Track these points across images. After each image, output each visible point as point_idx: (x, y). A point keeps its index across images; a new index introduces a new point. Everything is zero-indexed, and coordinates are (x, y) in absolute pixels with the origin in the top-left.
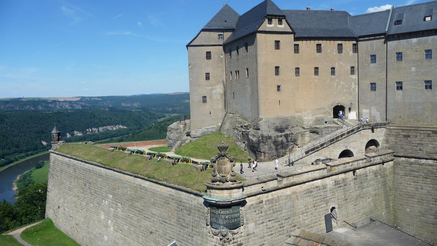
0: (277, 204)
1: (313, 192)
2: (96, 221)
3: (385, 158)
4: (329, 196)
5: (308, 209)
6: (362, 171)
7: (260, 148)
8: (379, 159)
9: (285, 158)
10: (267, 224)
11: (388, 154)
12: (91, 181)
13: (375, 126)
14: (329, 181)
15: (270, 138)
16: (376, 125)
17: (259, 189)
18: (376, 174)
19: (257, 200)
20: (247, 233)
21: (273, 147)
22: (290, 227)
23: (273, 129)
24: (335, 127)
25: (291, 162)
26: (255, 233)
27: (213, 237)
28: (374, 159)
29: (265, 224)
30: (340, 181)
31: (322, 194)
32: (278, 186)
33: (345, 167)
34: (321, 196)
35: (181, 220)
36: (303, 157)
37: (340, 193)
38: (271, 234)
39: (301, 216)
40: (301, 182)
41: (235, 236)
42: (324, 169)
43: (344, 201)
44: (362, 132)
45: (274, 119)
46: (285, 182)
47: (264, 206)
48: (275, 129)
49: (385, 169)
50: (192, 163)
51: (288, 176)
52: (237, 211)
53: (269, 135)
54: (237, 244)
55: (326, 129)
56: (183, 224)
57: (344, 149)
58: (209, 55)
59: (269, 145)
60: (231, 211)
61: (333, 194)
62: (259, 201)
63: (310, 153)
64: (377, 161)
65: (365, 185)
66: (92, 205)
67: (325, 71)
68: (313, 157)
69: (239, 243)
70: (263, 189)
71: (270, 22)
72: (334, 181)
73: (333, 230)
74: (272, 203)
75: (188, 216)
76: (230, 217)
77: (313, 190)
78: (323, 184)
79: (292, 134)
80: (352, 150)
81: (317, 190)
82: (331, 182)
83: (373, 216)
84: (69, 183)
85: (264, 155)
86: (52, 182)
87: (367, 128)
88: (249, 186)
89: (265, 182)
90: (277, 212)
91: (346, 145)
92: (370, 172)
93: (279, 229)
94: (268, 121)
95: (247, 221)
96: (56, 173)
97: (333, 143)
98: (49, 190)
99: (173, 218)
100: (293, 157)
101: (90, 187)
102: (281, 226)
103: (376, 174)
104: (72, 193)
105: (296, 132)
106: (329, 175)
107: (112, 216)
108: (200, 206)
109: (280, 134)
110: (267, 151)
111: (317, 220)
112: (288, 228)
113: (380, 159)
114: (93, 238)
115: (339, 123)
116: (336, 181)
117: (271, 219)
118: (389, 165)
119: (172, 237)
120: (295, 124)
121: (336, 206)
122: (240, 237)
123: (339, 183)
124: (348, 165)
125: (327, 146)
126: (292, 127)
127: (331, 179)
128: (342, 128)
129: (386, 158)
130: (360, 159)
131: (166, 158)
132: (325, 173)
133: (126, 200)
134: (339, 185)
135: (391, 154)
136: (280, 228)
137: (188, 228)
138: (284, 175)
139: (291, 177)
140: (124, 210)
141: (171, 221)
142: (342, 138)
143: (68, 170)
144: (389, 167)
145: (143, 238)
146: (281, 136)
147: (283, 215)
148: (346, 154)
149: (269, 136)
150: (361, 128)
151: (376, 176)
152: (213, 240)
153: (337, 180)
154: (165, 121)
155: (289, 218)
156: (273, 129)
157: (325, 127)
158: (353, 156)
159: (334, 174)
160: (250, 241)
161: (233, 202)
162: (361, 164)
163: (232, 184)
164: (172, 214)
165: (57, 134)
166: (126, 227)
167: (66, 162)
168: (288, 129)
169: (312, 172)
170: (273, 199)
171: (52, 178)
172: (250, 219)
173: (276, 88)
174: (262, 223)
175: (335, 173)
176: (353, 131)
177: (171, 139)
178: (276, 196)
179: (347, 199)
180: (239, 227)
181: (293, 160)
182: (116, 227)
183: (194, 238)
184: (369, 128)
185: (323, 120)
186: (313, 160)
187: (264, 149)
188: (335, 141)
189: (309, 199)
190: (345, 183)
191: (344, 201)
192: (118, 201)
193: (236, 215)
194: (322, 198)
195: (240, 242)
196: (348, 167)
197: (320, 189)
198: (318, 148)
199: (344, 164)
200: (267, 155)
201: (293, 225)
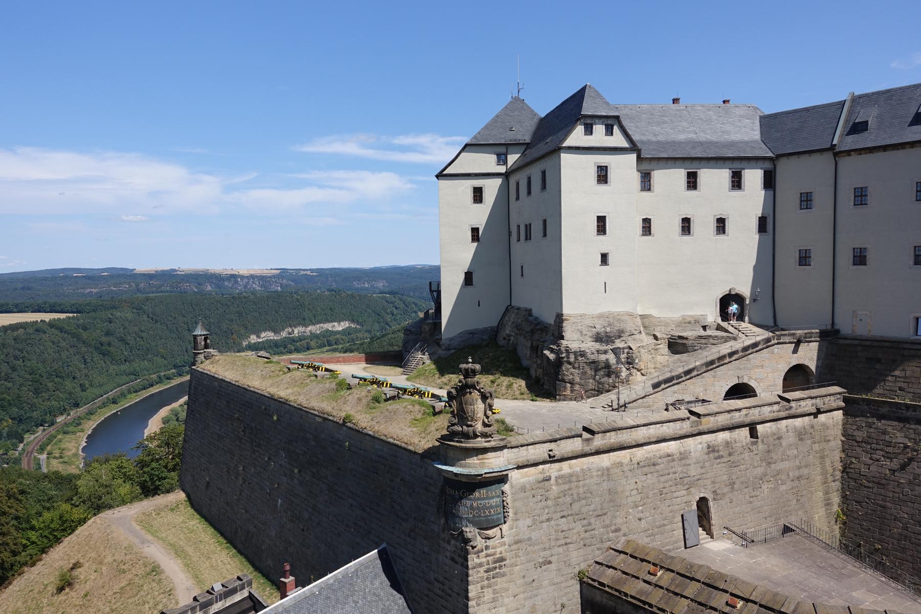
0: (581, 483)
1: (658, 464)
3: (824, 404)
4: (695, 474)
5: (648, 497)
6: (770, 428)
7: (564, 375)
8: (810, 405)
9: (612, 396)
10: (558, 523)
11: (830, 395)
13: (805, 338)
14: (695, 445)
15: (583, 354)
16: (808, 335)
17: (544, 453)
18: (802, 435)
19: (538, 474)
20: (516, 538)
21: (590, 372)
22: (608, 532)
24: (723, 337)
25: (622, 402)
26: (531, 539)
27: (449, 543)
28: (799, 404)
29: (553, 523)
30: (718, 446)
31: (680, 469)
32: (582, 450)
33: (732, 417)
34: (675, 473)
36: (648, 394)
37: (720, 471)
38: (566, 544)
39: (631, 510)
40: (634, 443)
41: (490, 543)
42: (683, 420)
43: (726, 485)
44: (776, 349)
45: (593, 318)
46: (599, 441)
47: (554, 487)
49: (824, 425)
50: (431, 397)
51: (605, 432)
52: (496, 493)
53: (582, 349)
54: (494, 558)
55: (703, 341)
57: (735, 381)
58: (478, 195)
59: (581, 367)
60: (483, 492)
61: (703, 471)
62: (541, 477)
63: (663, 386)
64: (806, 409)
65: (774, 456)
67: (704, 226)
68: (670, 394)
69: (498, 556)
70: (550, 453)
71: (589, 130)
73: (702, 542)
74: (570, 482)
76: (481, 504)
77: (660, 460)
78: (682, 449)
79: (631, 349)
80: (753, 384)
81: (669, 462)
82: (700, 446)
83: (793, 520)
85: (571, 387)
87: (787, 341)
88: (522, 446)
89: (555, 441)
90: (580, 500)
91: (740, 373)
92: (788, 431)
93: (583, 535)
94: (580, 322)
95: (516, 514)
96: (198, 409)
97: (711, 370)
100: (625, 394)
102: (589, 528)
103: (801, 435)
105: (639, 345)
106: (695, 433)
109: (604, 347)
110: (577, 379)
111: (665, 522)
112: (603, 534)
113: (812, 405)
115: (731, 329)
116: (711, 445)
117: (565, 513)
118: (833, 418)
121: (709, 496)
122: (501, 546)
123: (716, 449)
124: (737, 414)
125: (698, 375)
126: (630, 335)
127: (700, 440)
128: (735, 339)
129: (826, 403)
130: (764, 403)
131: (386, 386)
132: (686, 427)
134: (717, 454)
135: (838, 396)
136: (586, 531)
138: (595, 429)
139: (613, 433)
142: (731, 359)
144: (833, 422)
146: (605, 352)
147: (592, 507)
148: (740, 391)
149: (580, 351)
150: (774, 340)
151: (801, 440)
155: (605, 514)
156: (590, 337)
157: (701, 337)
158: (756, 396)
159: (706, 431)
160: (521, 554)
161: (487, 475)
162: (767, 412)
163: (486, 442)
165: (203, 337)
169: (658, 426)
170: (571, 475)
171: (191, 416)
172: (524, 510)
174: (548, 520)
175: (708, 429)
176: (755, 345)
178: (578, 469)
179: (734, 483)
180: (499, 525)
181: (627, 400)
184: (792, 340)
185: (696, 322)
186: (671, 400)
187: (571, 377)
188: (717, 365)
189: (651, 479)
190: (731, 450)
191: (728, 488)
193: (494, 502)
194: (678, 478)
195: (500, 554)
196: (738, 417)
197: (673, 460)
198: (679, 377)
199: (729, 412)
200: (577, 387)
201: (613, 528)
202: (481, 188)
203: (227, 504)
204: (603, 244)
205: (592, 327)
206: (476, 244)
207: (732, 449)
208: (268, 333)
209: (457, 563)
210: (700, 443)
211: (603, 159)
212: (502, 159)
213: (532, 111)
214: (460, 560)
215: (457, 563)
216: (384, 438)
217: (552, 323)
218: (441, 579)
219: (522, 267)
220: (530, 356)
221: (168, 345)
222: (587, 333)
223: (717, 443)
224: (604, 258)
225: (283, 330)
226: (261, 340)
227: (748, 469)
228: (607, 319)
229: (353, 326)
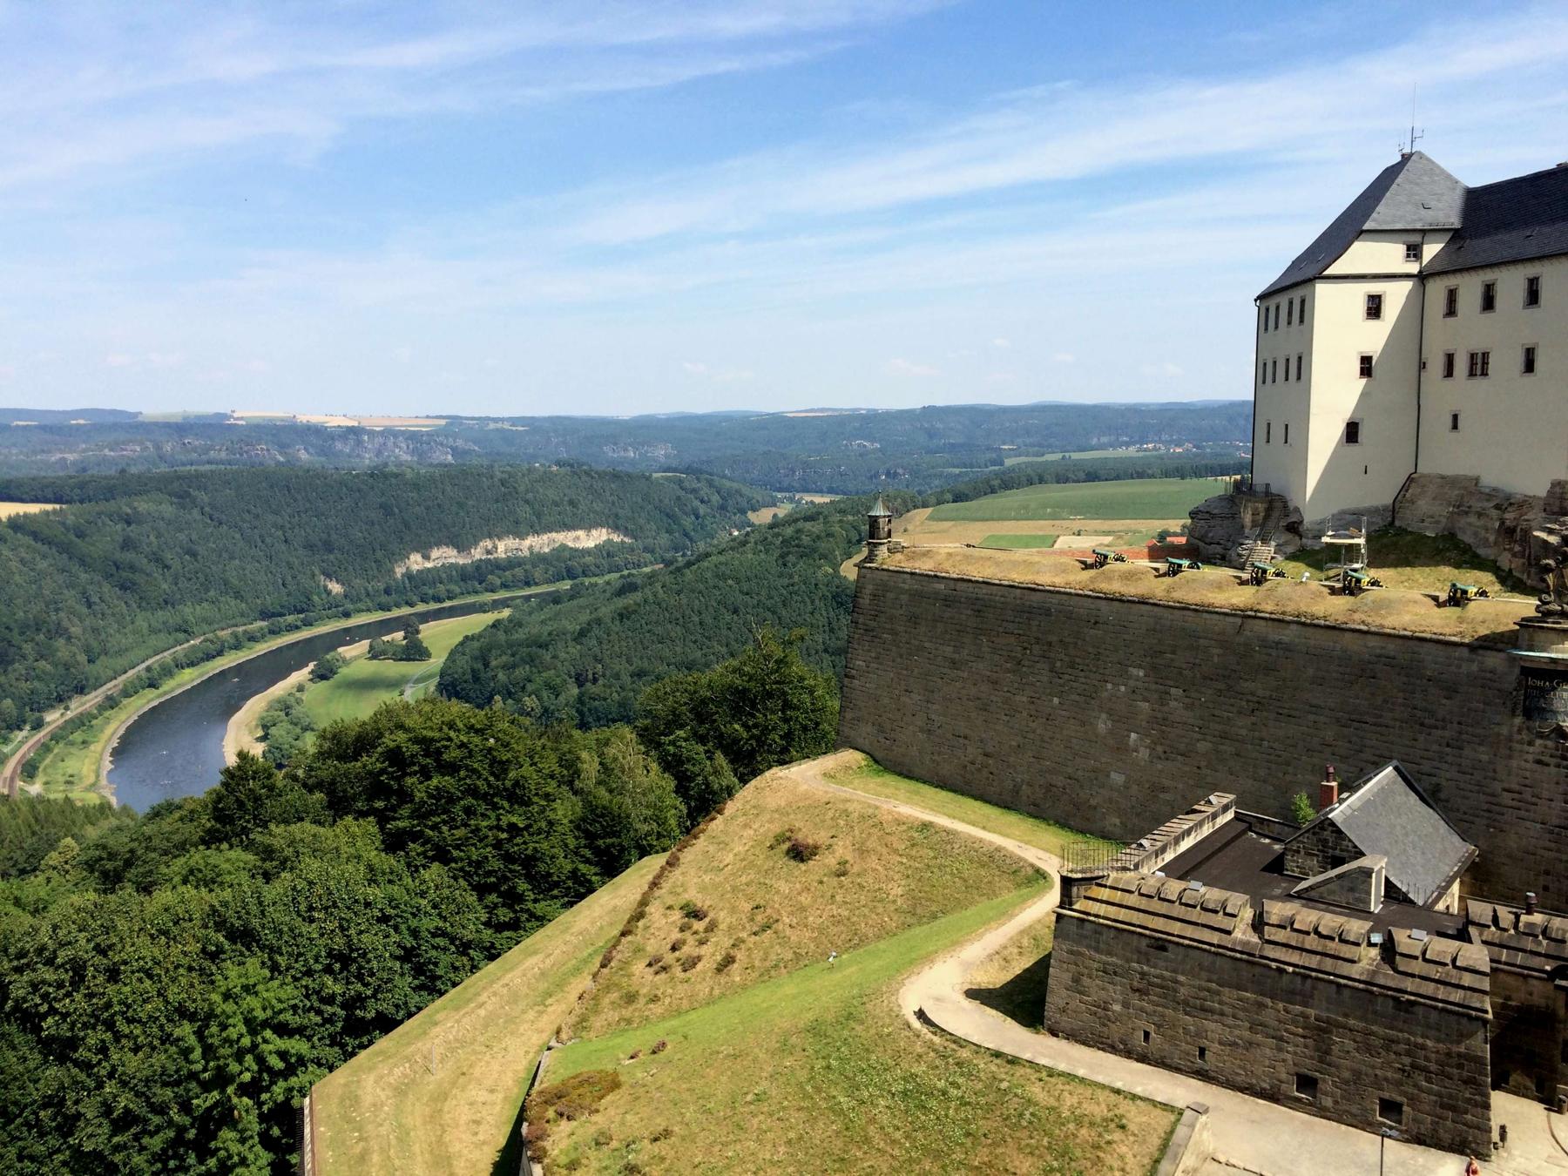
2: (1074, 741)
12: (1054, 639)
27: (1530, 743)
35: (1419, 714)
56: (1427, 721)
58: (1374, 308)
66: (1056, 700)
75: (1444, 701)
84: (951, 649)
86: (869, 651)
98: (854, 672)
99: (1392, 710)
101: (1052, 655)
104: (965, 675)
107: (1144, 723)
108: (1488, 675)
114: (1060, 784)
119: (1387, 754)
133: (1205, 678)
137: (1444, 728)
140: (1197, 703)
141: (1381, 716)
143: (947, 615)
145: (1273, 766)
152: (1531, 749)
154: (797, 520)
164: (1385, 701)
166: (1203, 746)
167: (937, 593)
177: (1218, 544)
182: (1160, 749)
183: (1467, 752)
192: (1171, 683)
202: (1379, 297)
203: (986, 755)
206: (1364, 381)
208: (446, 549)
209: (1547, 765)
212: (1414, 251)
213: (1449, 177)
214: (1553, 761)
215: (1547, 765)
216: (1392, 631)
217: (1542, 491)
218: (1515, 787)
219: (1455, 417)
220: (1495, 543)
221: (247, 572)
225: (476, 544)
226: (429, 565)
229: (626, 540)
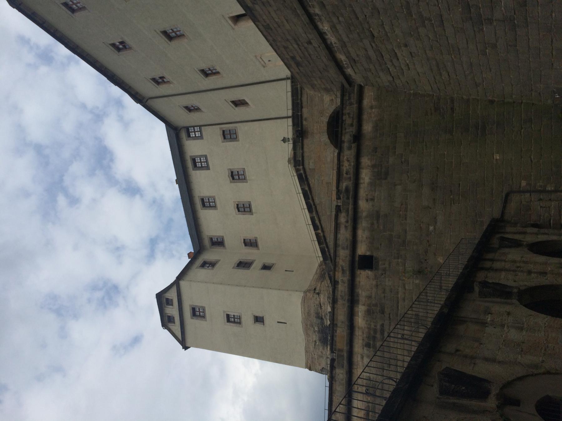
3: (352, 125)
6: (364, 230)
23: (323, 349)
28: (345, 175)
30: (369, 328)
48: (324, 344)
49: (376, 127)
72: (366, 350)
92: (373, 200)
120: (315, 297)
123: (372, 333)
126: (321, 307)
127: (359, 356)
134: (378, 336)
153: (365, 335)
168: (323, 317)
173: (258, 326)
179: (417, 315)
204: (247, 320)
205: (315, 345)
207: (376, 305)
210: (362, 358)
211: (187, 313)
222: (320, 350)
223: (367, 330)
224: (259, 320)
227: (404, 285)
228: (308, 326)
